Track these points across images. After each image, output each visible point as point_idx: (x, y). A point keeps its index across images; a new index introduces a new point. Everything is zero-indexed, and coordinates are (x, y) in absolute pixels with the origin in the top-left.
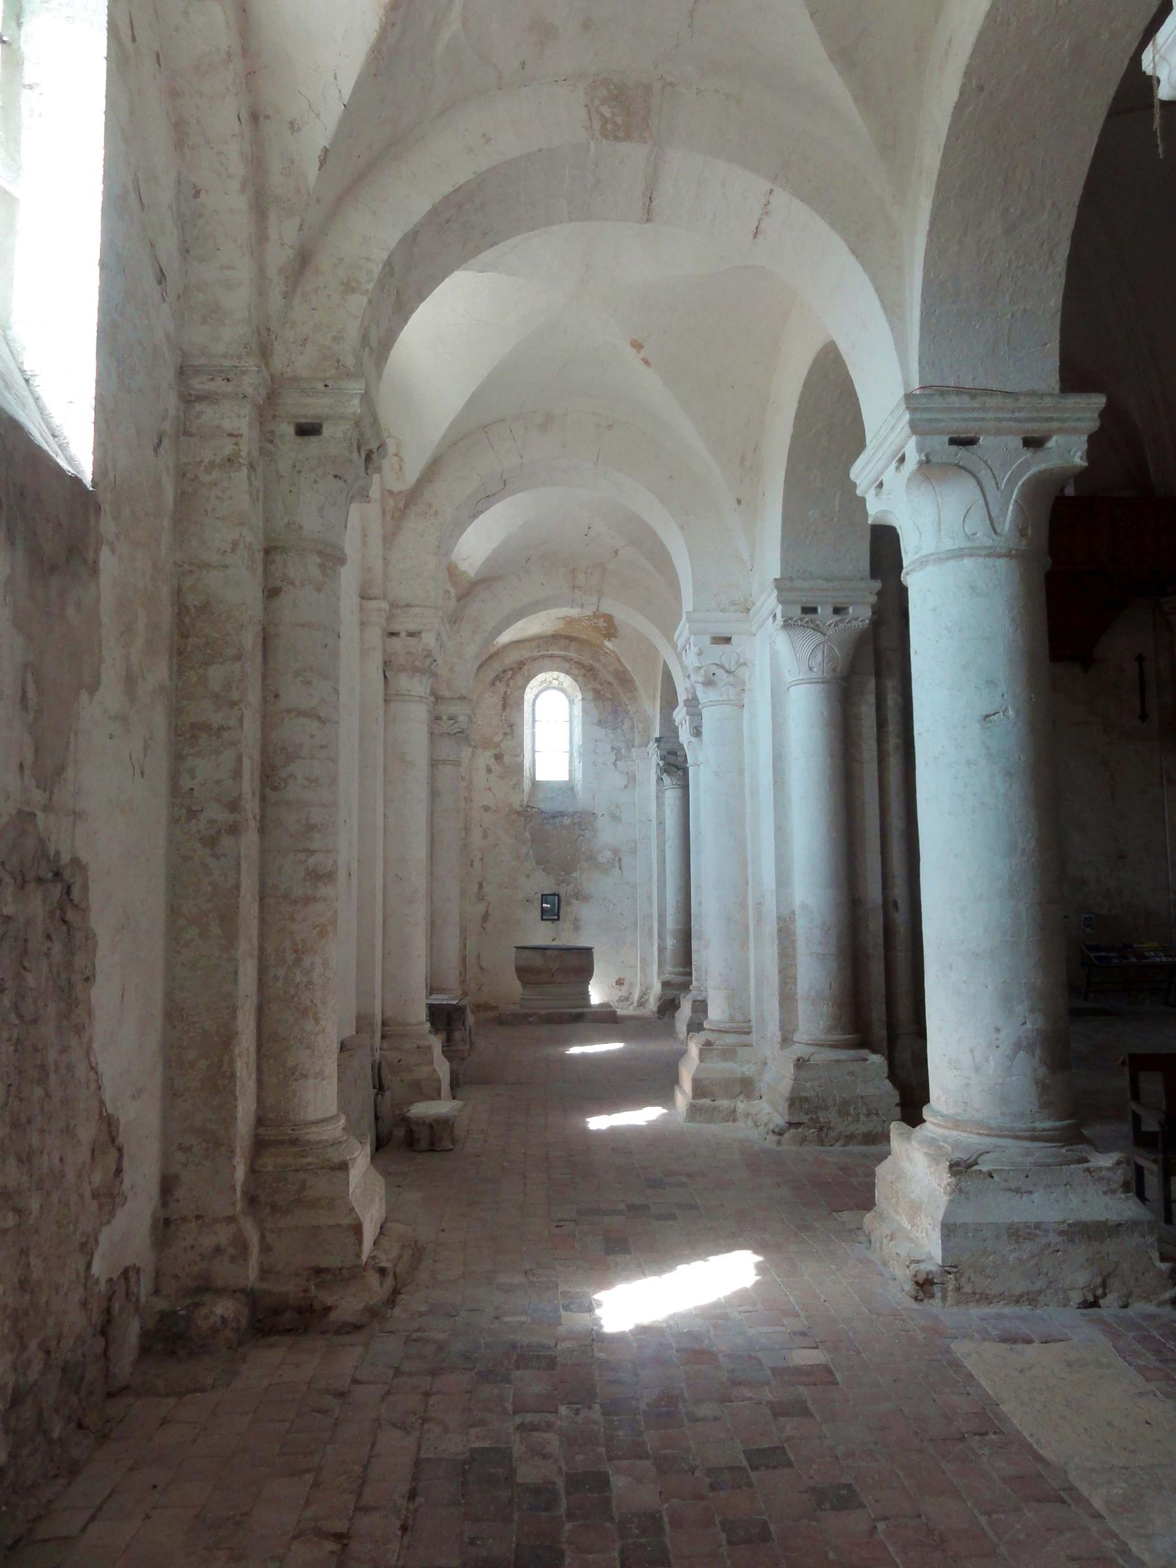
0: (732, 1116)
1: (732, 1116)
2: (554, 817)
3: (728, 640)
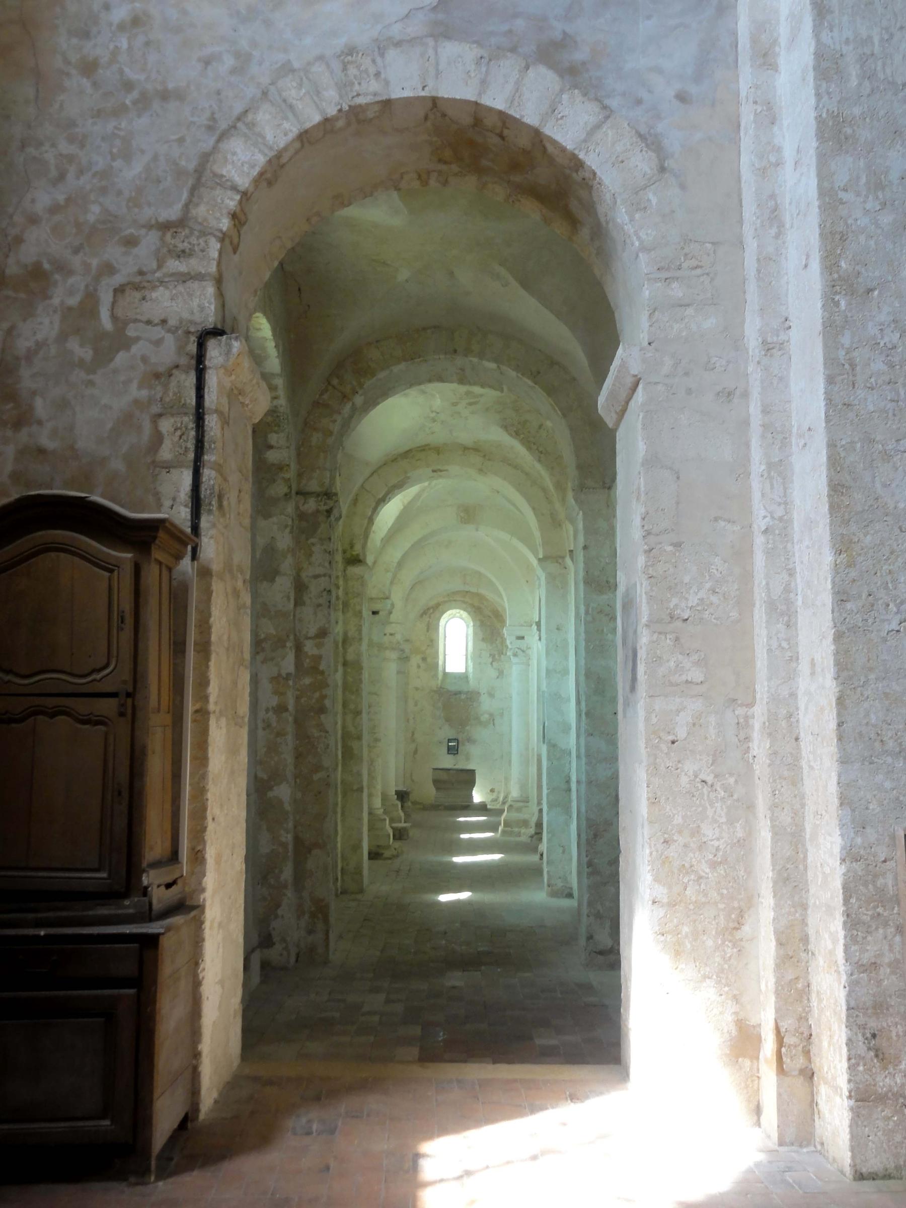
0: (519, 834)
1: (519, 834)
3: (523, 638)
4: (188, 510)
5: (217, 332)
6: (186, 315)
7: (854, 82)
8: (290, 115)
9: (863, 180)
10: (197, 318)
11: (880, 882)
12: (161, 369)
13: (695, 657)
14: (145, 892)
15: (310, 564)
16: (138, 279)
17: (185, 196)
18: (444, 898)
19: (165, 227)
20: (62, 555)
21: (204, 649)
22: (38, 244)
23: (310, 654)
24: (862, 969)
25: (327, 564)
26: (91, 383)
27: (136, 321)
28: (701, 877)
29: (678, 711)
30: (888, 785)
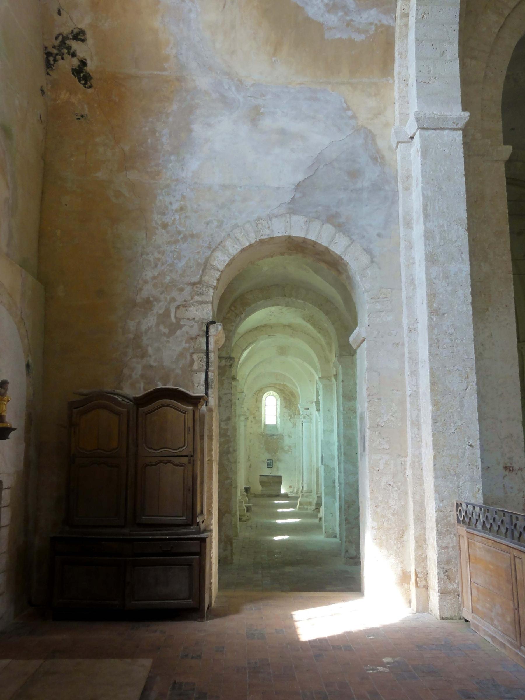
1: (307, 509)
2: (271, 436)
3: (308, 409)
4: (204, 387)
5: (213, 323)
6: (202, 317)
7: (438, 241)
8: (238, 243)
9: (441, 275)
10: (206, 317)
11: (449, 519)
12: (193, 336)
13: (386, 440)
14: (198, 524)
15: (223, 388)
16: (184, 303)
17: (200, 272)
18: (276, 538)
19: (194, 284)
20: (169, 408)
21: (211, 438)
22: (148, 291)
23: (223, 428)
24: (442, 548)
25: (230, 388)
26: (168, 342)
27: (184, 319)
28: (389, 519)
29: (380, 459)
30: (451, 485)
